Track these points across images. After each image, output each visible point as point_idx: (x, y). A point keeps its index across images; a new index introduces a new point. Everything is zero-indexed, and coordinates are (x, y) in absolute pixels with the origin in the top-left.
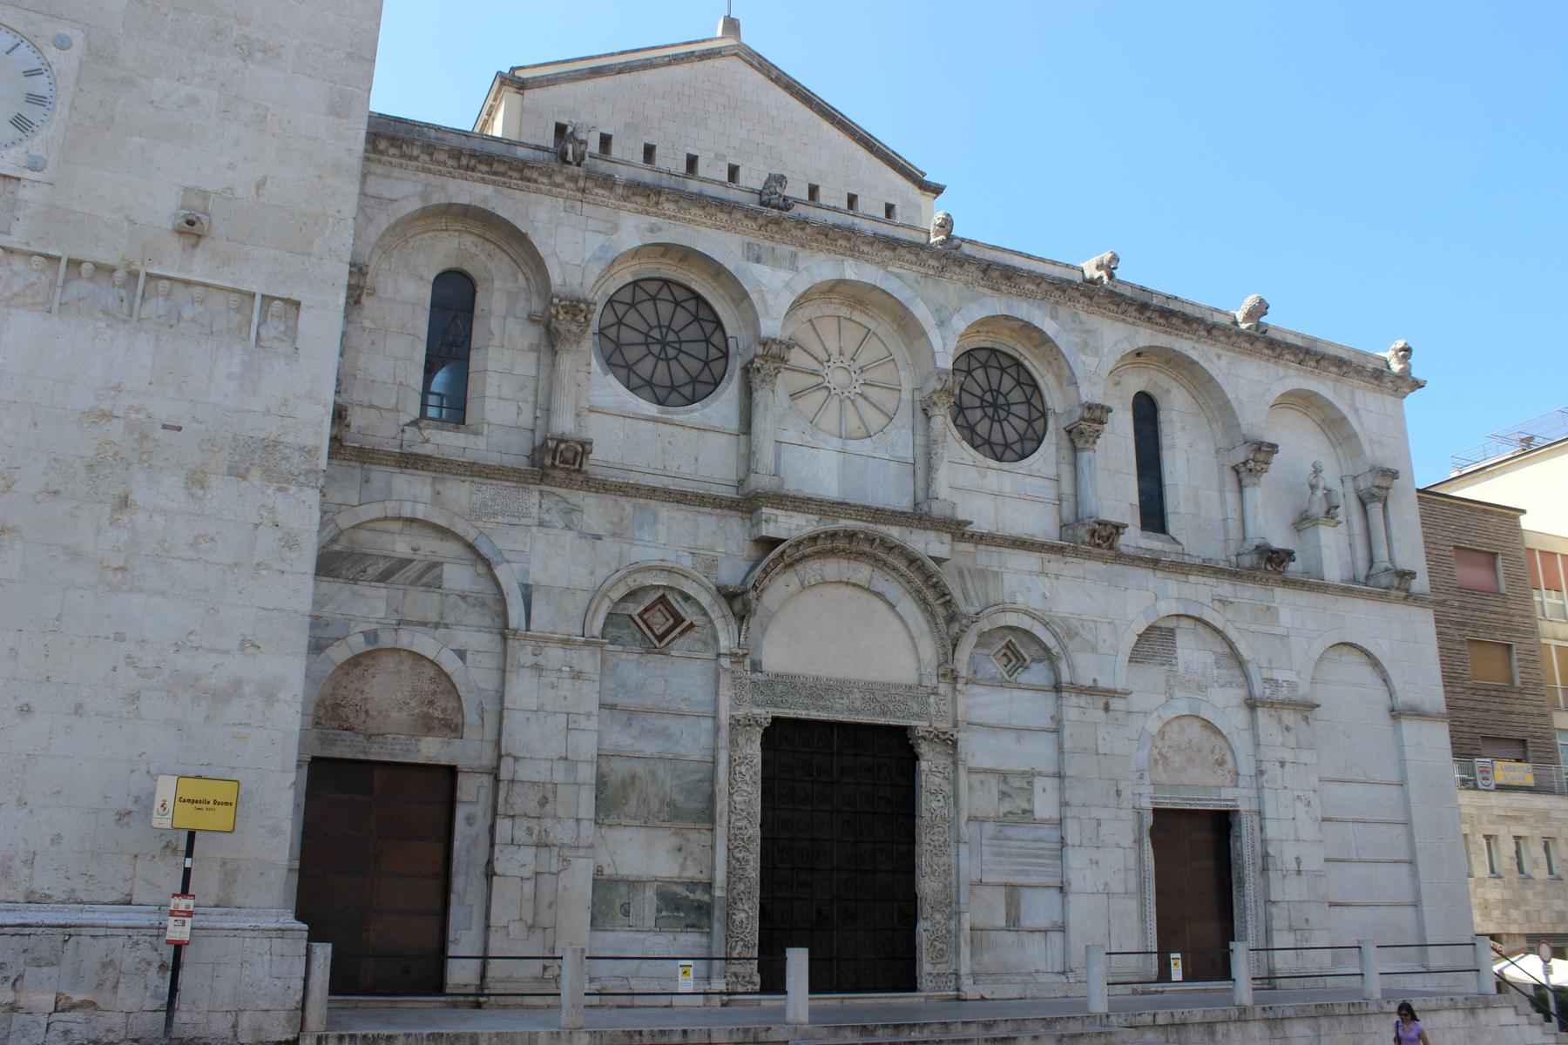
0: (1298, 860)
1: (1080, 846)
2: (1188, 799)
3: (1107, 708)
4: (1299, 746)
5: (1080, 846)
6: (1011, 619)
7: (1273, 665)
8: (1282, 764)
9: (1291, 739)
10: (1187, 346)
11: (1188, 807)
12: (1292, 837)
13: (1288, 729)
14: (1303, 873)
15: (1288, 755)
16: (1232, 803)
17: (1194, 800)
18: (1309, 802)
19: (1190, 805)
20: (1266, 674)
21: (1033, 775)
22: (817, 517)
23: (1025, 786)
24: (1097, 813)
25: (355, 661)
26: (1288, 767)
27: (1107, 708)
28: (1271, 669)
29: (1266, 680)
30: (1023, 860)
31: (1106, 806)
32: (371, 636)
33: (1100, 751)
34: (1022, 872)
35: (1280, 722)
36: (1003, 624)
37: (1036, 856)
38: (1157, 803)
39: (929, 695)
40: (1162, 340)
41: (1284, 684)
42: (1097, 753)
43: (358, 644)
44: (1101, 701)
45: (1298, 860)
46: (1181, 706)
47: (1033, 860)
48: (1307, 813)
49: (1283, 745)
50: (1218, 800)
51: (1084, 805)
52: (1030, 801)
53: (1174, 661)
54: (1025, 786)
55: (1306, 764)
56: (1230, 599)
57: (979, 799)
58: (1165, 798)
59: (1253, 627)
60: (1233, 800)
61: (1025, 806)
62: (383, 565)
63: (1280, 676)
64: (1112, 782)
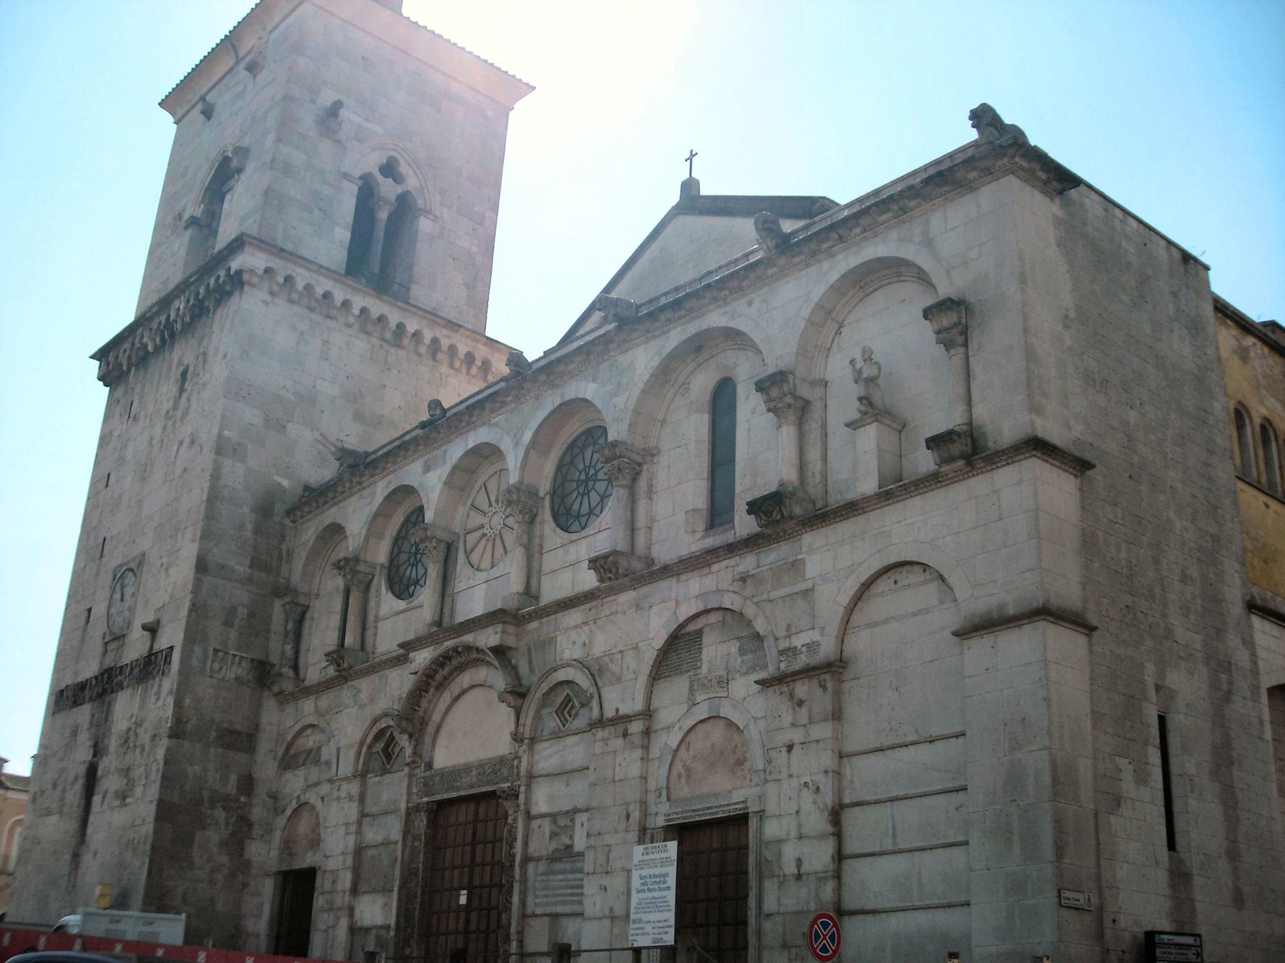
0: (799, 862)
1: (594, 873)
2: (698, 810)
3: (625, 735)
4: (811, 721)
5: (594, 873)
6: (561, 675)
7: (793, 630)
8: (790, 748)
9: (803, 712)
10: (716, 319)
11: (698, 819)
12: (793, 834)
13: (800, 703)
14: (804, 878)
15: (796, 736)
16: (741, 806)
17: (703, 809)
18: (818, 789)
19: (700, 815)
20: (783, 644)
21: (575, 813)
22: (432, 647)
23: (569, 823)
24: (609, 839)
25: (295, 810)
26: (796, 750)
27: (625, 735)
28: (789, 637)
29: (781, 653)
30: (563, 891)
31: (616, 832)
32: (298, 798)
33: (616, 778)
34: (564, 903)
35: (792, 695)
36: (555, 682)
37: (572, 887)
38: (669, 820)
39: (513, 760)
40: (676, 336)
41: (804, 649)
42: (614, 781)
43: (294, 804)
44: (620, 728)
45: (799, 862)
46: (702, 712)
47: (569, 891)
48: (815, 803)
49: (793, 724)
50: (727, 805)
51: (599, 834)
52: (571, 838)
53: (698, 664)
54: (569, 823)
55: (818, 741)
56: (753, 572)
57: (541, 842)
58: (677, 813)
59: (775, 594)
60: (743, 802)
61: (568, 841)
62: (303, 756)
63: (799, 641)
64: (625, 806)
